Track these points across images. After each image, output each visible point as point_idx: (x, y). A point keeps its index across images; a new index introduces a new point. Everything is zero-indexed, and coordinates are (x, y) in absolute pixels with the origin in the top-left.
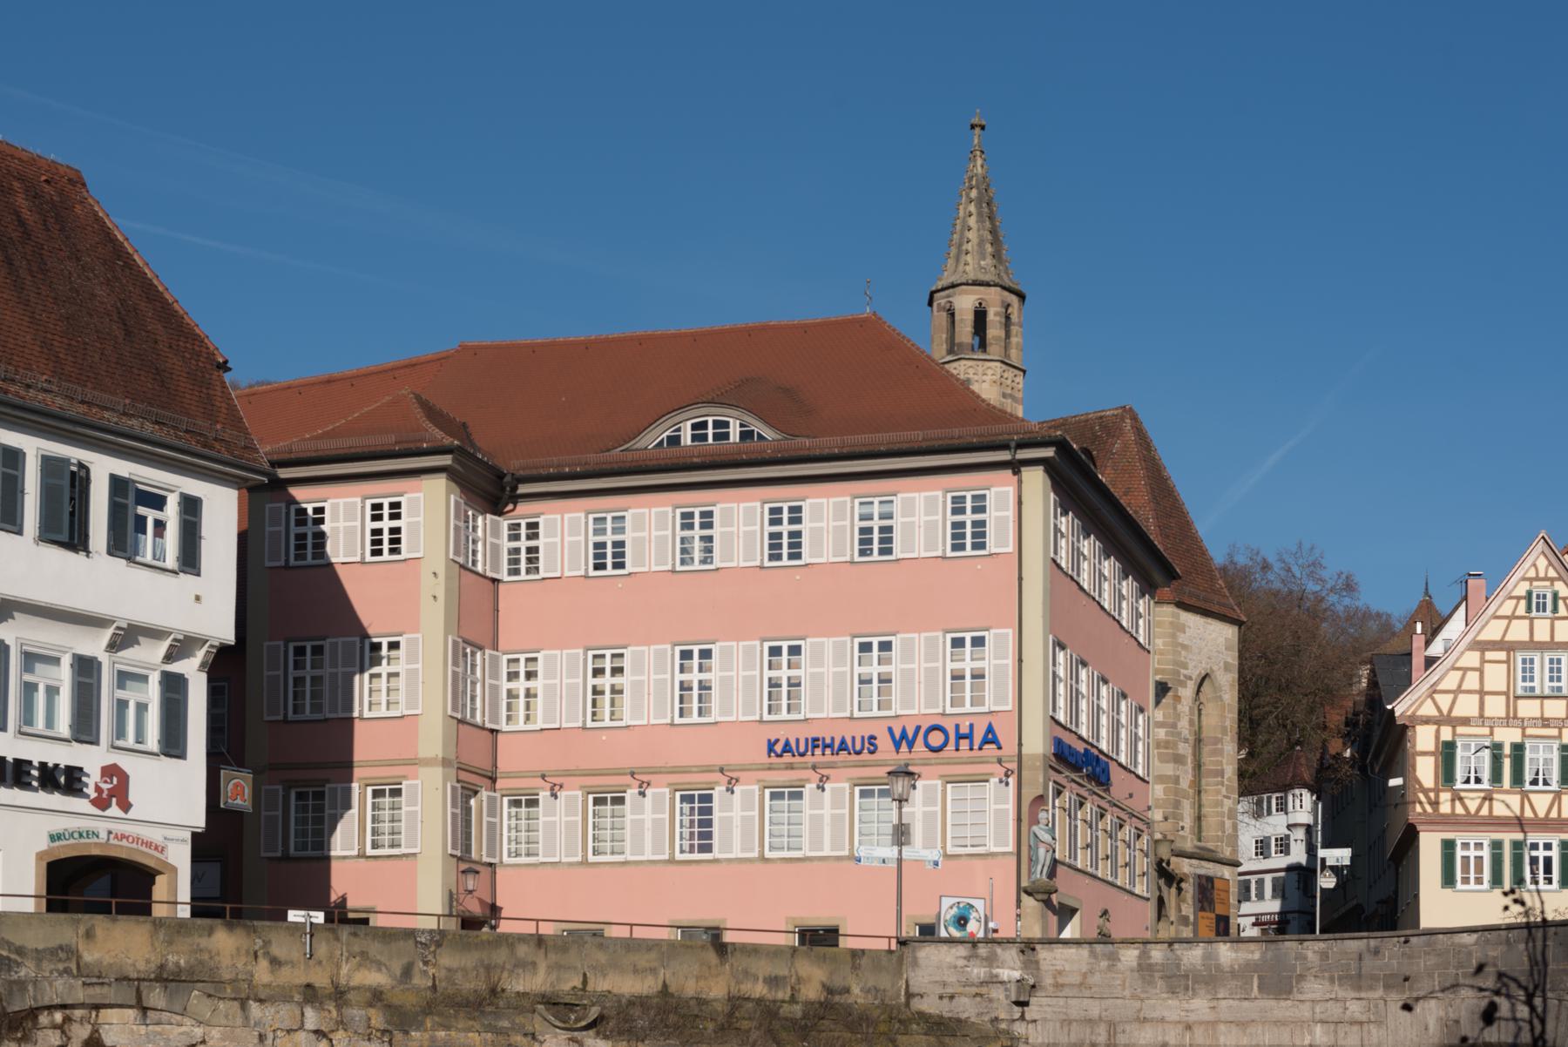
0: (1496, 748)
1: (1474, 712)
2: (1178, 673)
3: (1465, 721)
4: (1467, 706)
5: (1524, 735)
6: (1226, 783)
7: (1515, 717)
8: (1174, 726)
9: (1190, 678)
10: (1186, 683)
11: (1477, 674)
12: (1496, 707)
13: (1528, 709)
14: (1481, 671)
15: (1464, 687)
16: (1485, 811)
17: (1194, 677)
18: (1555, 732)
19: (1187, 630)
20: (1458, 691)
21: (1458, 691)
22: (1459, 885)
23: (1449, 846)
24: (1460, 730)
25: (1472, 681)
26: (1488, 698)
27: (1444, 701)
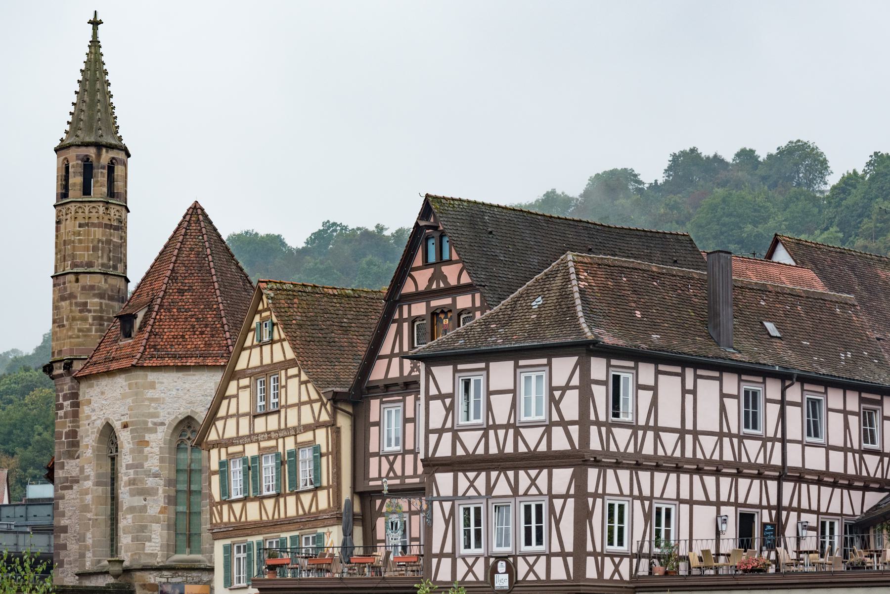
0: (245, 461)
1: (234, 435)
2: (146, 423)
3: (230, 442)
7: (254, 434)
8: (142, 466)
9: (163, 424)
10: (156, 429)
11: (236, 399)
13: (260, 425)
14: (236, 396)
15: (230, 413)
17: (167, 422)
18: (272, 443)
19: (157, 386)
22: (236, 585)
23: (228, 550)
24: (232, 449)
27: (220, 424)
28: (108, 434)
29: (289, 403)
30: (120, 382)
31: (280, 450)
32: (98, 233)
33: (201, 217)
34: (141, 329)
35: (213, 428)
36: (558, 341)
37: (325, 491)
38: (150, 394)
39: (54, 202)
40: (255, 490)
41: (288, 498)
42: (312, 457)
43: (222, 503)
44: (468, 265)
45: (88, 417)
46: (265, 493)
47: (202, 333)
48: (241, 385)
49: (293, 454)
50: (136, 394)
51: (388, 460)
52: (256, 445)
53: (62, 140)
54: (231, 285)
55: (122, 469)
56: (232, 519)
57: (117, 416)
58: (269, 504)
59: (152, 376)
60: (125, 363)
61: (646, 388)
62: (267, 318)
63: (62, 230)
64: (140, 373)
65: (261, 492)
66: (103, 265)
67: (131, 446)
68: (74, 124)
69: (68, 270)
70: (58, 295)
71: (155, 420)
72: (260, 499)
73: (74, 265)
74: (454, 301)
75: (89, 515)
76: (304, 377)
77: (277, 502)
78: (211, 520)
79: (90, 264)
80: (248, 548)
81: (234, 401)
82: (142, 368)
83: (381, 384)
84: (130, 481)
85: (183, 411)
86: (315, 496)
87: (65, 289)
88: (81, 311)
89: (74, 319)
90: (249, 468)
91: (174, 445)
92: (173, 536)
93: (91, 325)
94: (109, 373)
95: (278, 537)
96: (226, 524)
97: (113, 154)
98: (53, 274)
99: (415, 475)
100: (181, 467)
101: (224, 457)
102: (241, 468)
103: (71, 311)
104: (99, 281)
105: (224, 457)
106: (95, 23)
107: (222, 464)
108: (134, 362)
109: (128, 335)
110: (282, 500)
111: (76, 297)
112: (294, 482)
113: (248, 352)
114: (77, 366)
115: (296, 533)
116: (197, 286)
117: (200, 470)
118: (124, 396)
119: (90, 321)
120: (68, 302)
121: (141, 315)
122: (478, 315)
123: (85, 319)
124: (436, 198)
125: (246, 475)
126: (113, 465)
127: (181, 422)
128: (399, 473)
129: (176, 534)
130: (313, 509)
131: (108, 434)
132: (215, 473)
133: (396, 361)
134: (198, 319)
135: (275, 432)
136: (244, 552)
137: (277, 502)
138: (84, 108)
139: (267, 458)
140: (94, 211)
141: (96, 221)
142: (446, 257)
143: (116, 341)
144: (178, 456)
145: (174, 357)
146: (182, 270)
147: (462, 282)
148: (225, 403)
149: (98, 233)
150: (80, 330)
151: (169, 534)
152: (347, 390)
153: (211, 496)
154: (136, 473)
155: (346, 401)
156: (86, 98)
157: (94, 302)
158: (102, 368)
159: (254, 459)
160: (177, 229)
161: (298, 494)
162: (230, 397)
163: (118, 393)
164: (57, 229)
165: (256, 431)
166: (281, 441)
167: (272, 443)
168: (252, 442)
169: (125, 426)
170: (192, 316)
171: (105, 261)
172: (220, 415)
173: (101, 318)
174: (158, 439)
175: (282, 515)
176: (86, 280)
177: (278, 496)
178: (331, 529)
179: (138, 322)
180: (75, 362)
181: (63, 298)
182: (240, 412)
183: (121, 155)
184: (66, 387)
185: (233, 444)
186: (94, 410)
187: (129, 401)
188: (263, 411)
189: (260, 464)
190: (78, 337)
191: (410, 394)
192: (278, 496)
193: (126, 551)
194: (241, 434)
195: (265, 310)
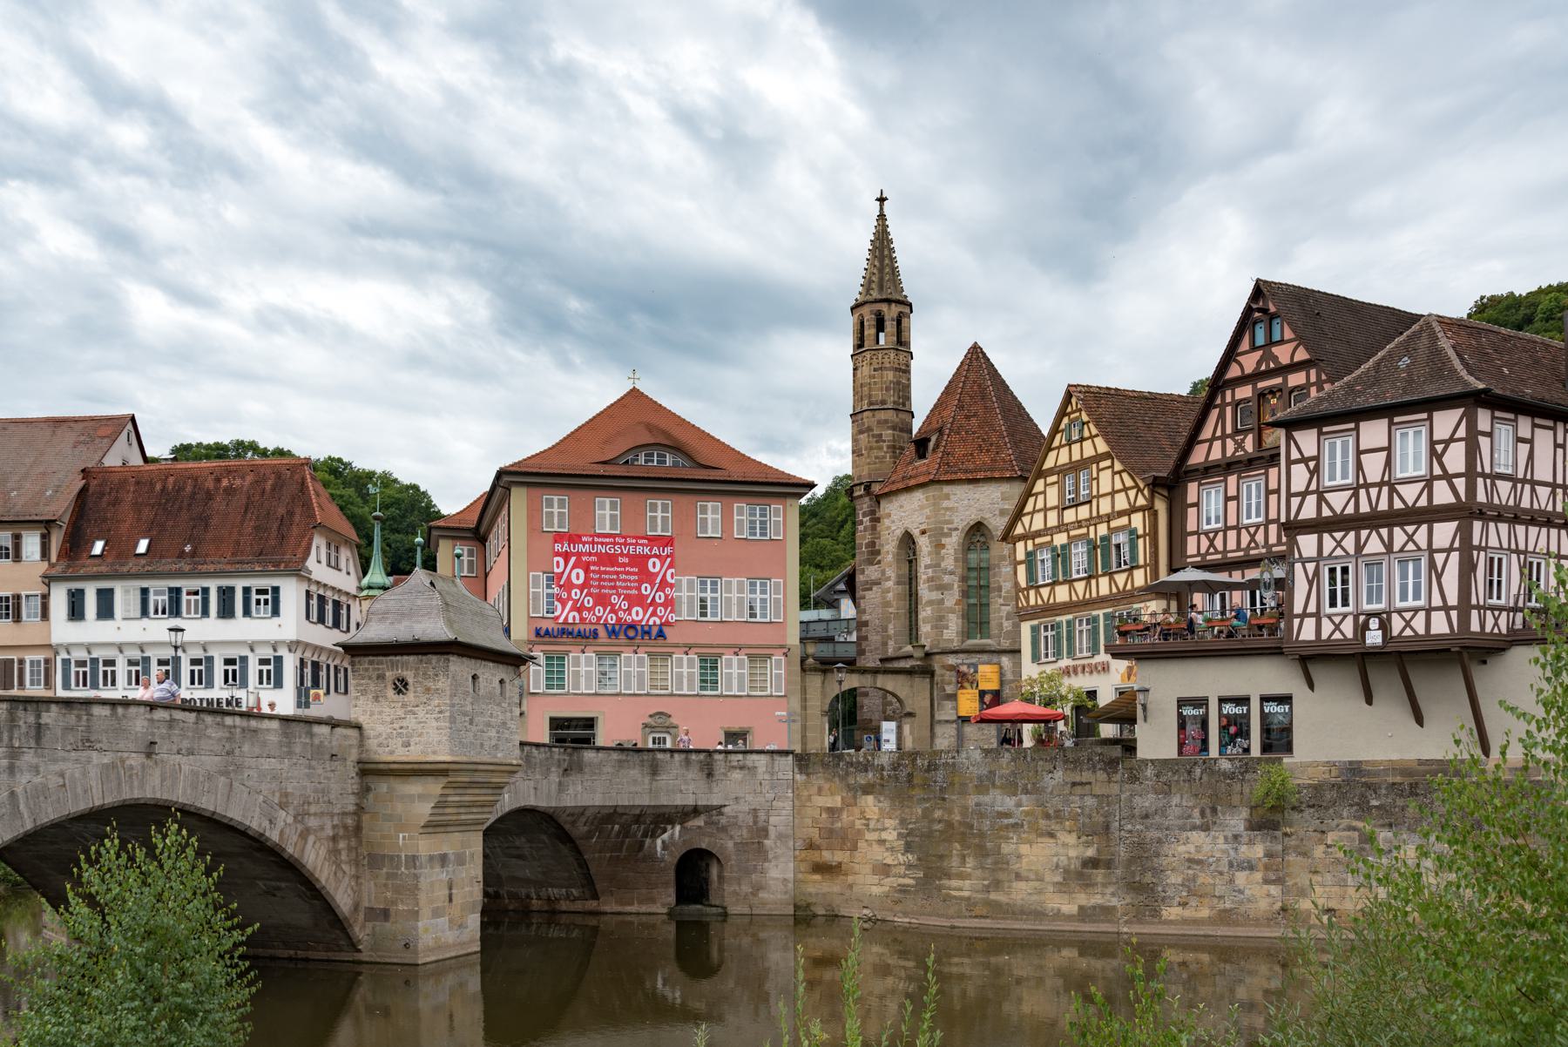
0: (1054, 549)
1: (1041, 526)
3: (1039, 534)
4: (1038, 524)
5: (1069, 537)
6: (1003, 594)
7: (1063, 525)
9: (956, 529)
12: (1053, 519)
13: (1069, 516)
14: (1044, 493)
16: (1051, 601)
17: (960, 527)
18: (1084, 531)
19: (952, 497)
20: (1034, 511)
21: (1034, 511)
23: (1035, 630)
24: (1038, 541)
25: (1040, 505)
26: (1049, 513)
27: (1026, 520)
28: (908, 541)
29: (1101, 493)
30: (918, 497)
31: (1092, 535)
32: (890, 375)
33: (980, 355)
34: (934, 450)
35: (1020, 523)
36: (1441, 393)
37: (1142, 570)
38: (945, 504)
39: (852, 352)
40: (1065, 573)
41: (1100, 579)
42: (1127, 540)
43: (1028, 588)
44: (1301, 340)
45: (889, 528)
46: (1075, 576)
47: (988, 451)
48: (1048, 482)
49: (1105, 539)
50: (934, 504)
51: (1208, 538)
52: (1066, 534)
53: (856, 300)
54: (1009, 411)
55: (921, 569)
56: (1040, 602)
57: (915, 525)
58: (1080, 586)
59: (947, 489)
60: (922, 480)
61: (1523, 441)
62: (1077, 418)
63: (859, 374)
64: (938, 486)
65: (1071, 576)
66: (894, 402)
67: (929, 549)
68: (867, 286)
69: (865, 407)
70: (856, 429)
71: (950, 526)
72: (1071, 582)
73: (871, 404)
74: (1286, 381)
75: (891, 610)
76: (1118, 466)
77: (1088, 584)
78: (1017, 604)
79: (883, 402)
80: (1059, 625)
81: (1041, 498)
82: (939, 482)
83: (1200, 467)
84: (928, 578)
85: (973, 517)
86: (1131, 575)
87: (863, 424)
88: (877, 442)
89: (871, 448)
90: (1058, 556)
91: (966, 547)
92: (966, 625)
93: (886, 453)
94: (908, 489)
95: (1090, 615)
96: (1032, 606)
97: (901, 308)
98: (851, 412)
99: (1239, 548)
100: (972, 566)
101: (1030, 548)
102: (1049, 556)
103: (869, 442)
104: (890, 415)
105: (1030, 548)
106: (882, 200)
107: (1028, 554)
108: (932, 477)
109: (922, 456)
110: (1093, 582)
111: (872, 430)
112: (1106, 564)
113: (1055, 452)
114: (876, 488)
115: (1110, 610)
116: (981, 412)
117: (988, 568)
118: (922, 508)
119: (885, 449)
120: (866, 435)
121: (934, 439)
122: (1313, 390)
123: (880, 448)
124: (1265, 282)
125: (1054, 561)
126: (910, 567)
127: (972, 527)
128: (1220, 548)
129: (969, 623)
130: (1129, 587)
131: (908, 541)
132: (1021, 562)
133: (1217, 445)
134: (984, 440)
135: (1086, 520)
136: (1052, 630)
137: (1088, 584)
138: (875, 271)
139: (1076, 545)
140: (886, 357)
141: (888, 365)
142: (1276, 337)
143: (911, 463)
144: (969, 556)
145: (966, 471)
146: (968, 399)
147: (1296, 359)
148: (1031, 500)
149: (890, 375)
150: (876, 458)
151: (963, 623)
152: (1165, 475)
153: (1017, 584)
154: (934, 572)
155: (1163, 486)
156: (877, 263)
157: (888, 434)
158: (901, 486)
159: (1063, 547)
160: (960, 367)
161: (1111, 575)
162: (1037, 495)
163: (916, 505)
164: (854, 376)
165: (1066, 521)
166: (1092, 528)
167: (1084, 531)
168: (1060, 532)
169: (923, 532)
170: (978, 438)
171: (896, 399)
172: (1026, 511)
173: (894, 447)
174: (953, 542)
175: (1094, 595)
176: (882, 415)
177: (1089, 578)
178: (1148, 604)
179: (931, 445)
180: (873, 485)
181: (861, 432)
182: (1048, 505)
183: (907, 310)
184: (865, 506)
185: (1040, 536)
186: (893, 522)
187: (928, 510)
188: (1072, 504)
189: (1070, 550)
190: (875, 463)
191: (1232, 474)
192: (1089, 578)
193: (926, 638)
194: (1049, 525)
195: (1073, 412)
